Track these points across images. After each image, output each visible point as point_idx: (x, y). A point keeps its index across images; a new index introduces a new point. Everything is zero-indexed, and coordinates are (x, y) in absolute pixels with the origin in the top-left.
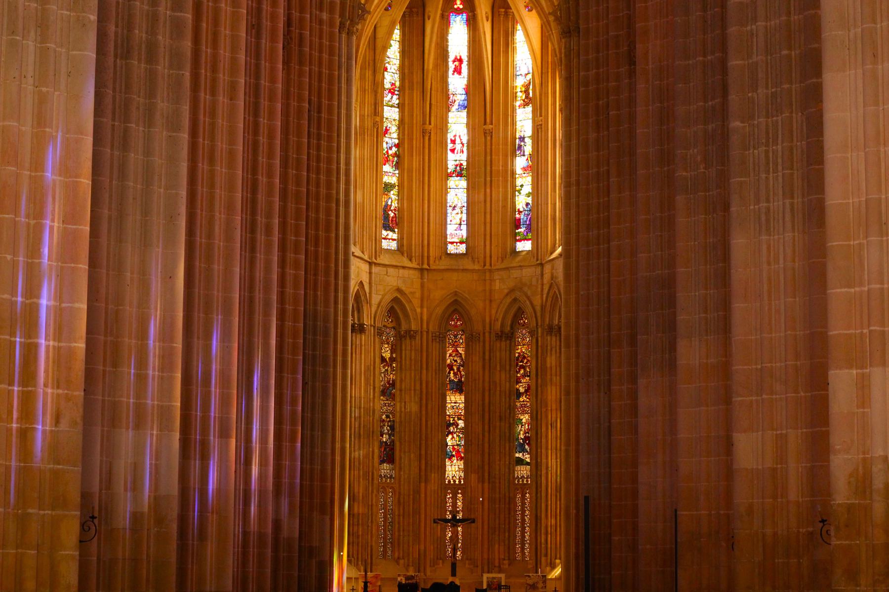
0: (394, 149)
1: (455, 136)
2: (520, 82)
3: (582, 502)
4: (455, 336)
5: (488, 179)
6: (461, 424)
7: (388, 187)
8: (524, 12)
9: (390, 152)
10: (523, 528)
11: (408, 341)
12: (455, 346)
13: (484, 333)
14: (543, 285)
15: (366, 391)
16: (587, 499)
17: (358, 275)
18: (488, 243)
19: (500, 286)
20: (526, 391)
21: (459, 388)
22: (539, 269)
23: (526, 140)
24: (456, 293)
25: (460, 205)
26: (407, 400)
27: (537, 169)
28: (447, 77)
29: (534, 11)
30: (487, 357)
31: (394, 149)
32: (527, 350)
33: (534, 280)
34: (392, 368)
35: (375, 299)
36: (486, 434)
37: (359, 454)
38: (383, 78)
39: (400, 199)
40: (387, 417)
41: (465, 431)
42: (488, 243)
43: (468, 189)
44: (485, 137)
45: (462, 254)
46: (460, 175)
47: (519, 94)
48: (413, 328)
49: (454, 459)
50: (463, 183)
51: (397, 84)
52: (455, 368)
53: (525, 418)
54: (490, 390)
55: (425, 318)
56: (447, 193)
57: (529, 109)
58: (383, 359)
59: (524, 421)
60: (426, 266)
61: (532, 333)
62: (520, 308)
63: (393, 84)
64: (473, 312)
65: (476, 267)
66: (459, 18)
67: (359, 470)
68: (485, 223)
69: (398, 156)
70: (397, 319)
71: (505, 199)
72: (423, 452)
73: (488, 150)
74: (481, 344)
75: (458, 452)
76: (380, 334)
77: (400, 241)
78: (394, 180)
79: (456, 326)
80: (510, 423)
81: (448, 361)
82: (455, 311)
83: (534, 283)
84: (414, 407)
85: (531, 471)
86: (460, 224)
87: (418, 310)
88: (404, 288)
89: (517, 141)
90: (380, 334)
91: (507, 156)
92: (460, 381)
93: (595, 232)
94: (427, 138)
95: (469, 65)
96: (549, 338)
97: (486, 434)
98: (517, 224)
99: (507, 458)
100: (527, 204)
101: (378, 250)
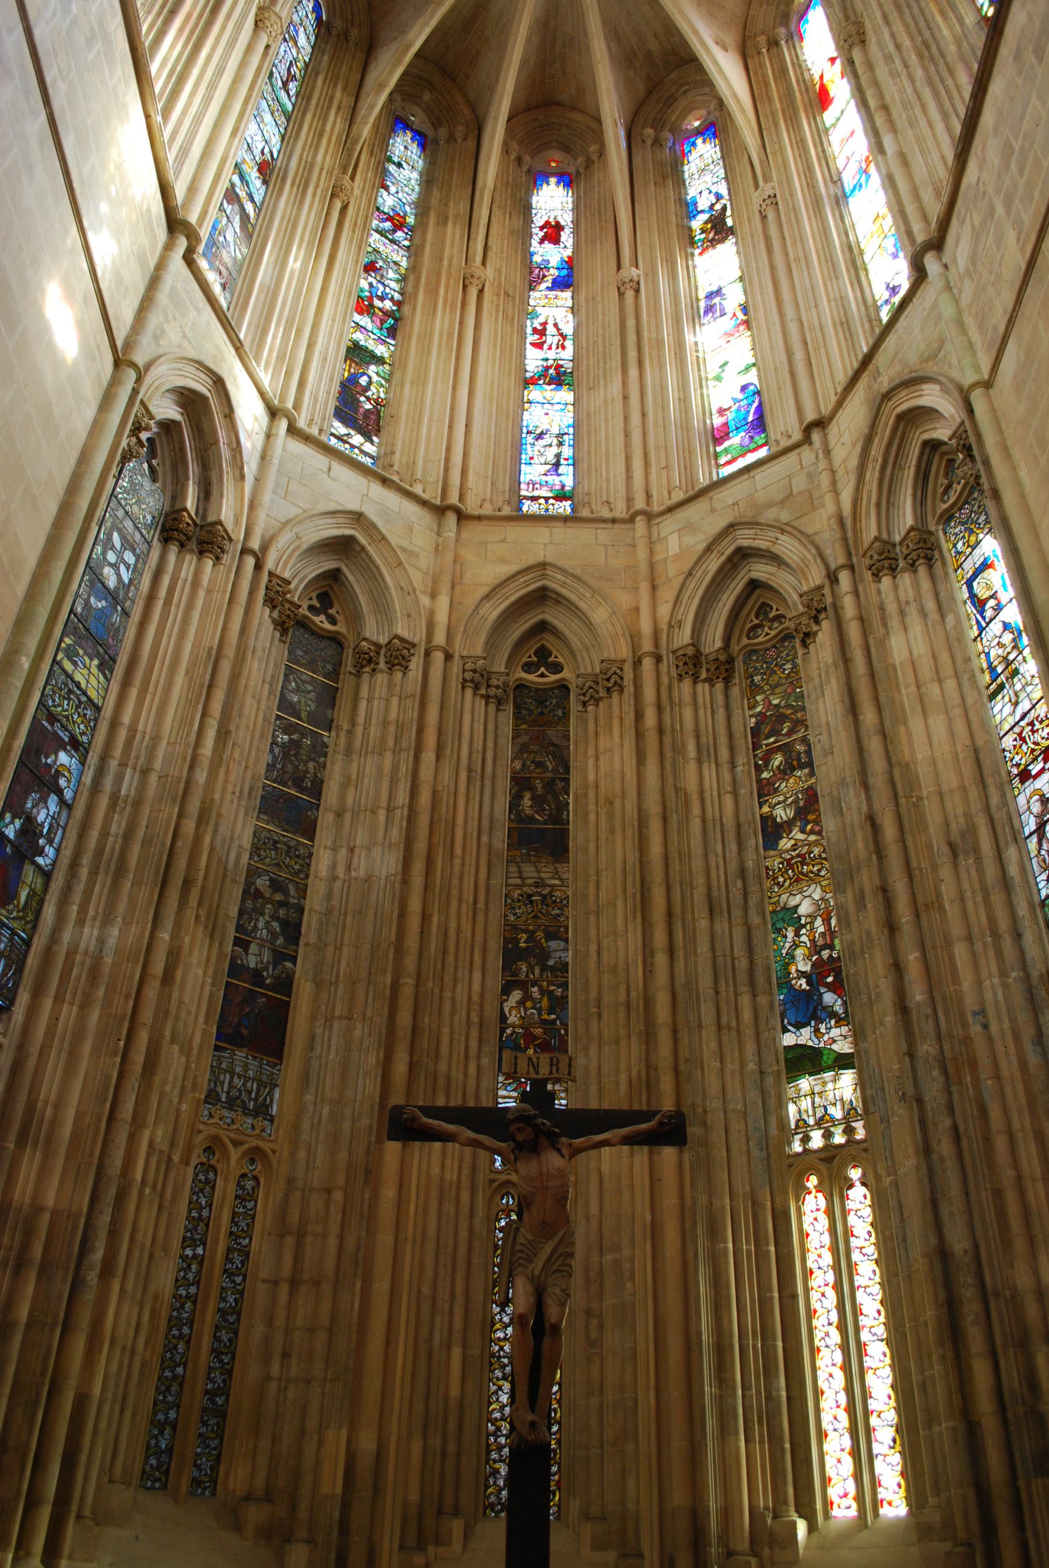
1: (545, 324)
4: (541, 702)
5: (632, 354)
9: (377, 303)
11: (381, 678)
13: (637, 663)
14: (833, 472)
22: (807, 454)
23: (724, 291)
25: (555, 430)
26: (361, 837)
31: (388, 305)
32: (786, 696)
36: (661, 959)
40: (276, 885)
44: (621, 295)
51: (411, 220)
52: (538, 784)
54: (665, 819)
55: (442, 617)
57: (728, 249)
59: (805, 909)
60: (453, 499)
62: (754, 585)
64: (599, 615)
65: (606, 514)
67: (85, 1007)
69: (396, 320)
70: (355, 619)
72: (404, 1019)
73: (630, 310)
74: (629, 690)
78: (380, 350)
80: (749, 929)
83: (799, 484)
86: (557, 465)
87: (425, 601)
89: (702, 304)
94: (473, 292)
96: (886, 581)
97: (661, 959)
99: (750, 1048)
100: (744, 388)
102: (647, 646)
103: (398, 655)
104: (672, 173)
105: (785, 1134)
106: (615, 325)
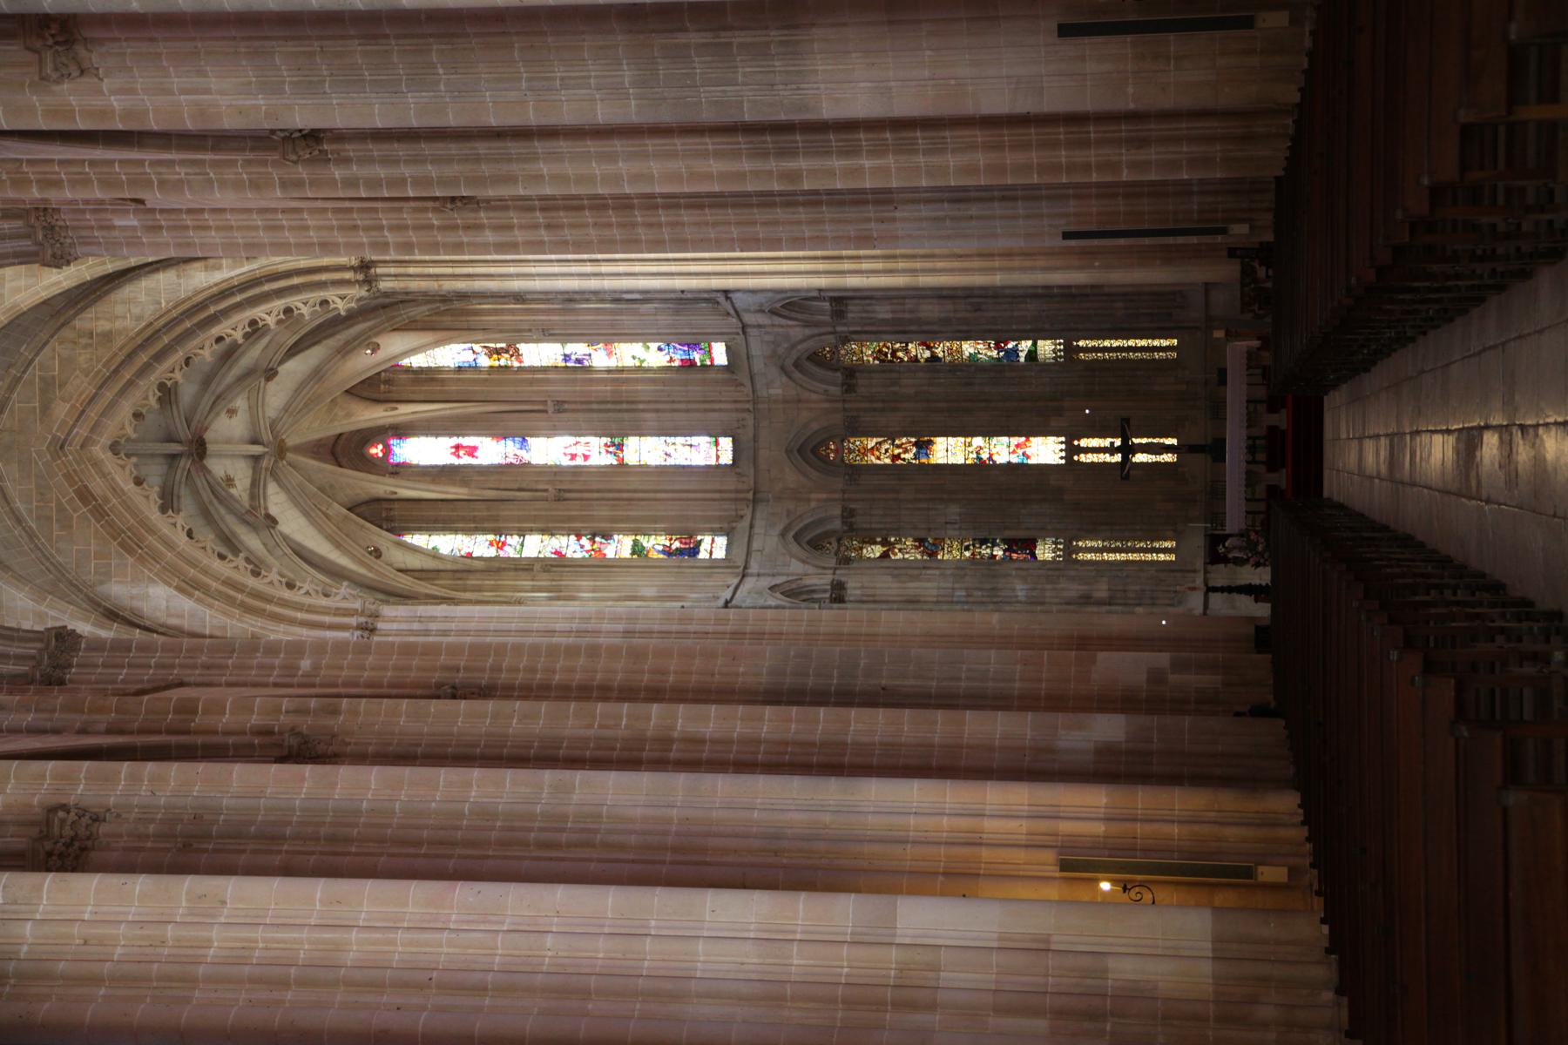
0: (584, 541)
2: (484, 362)
3: (1073, 243)
5: (624, 406)
6: (978, 441)
7: (637, 549)
8: (381, 355)
9: (588, 547)
10: (1130, 349)
12: (866, 451)
13: (845, 410)
15: (929, 580)
16: (1067, 235)
17: (760, 593)
18: (717, 406)
19: (776, 387)
20: (929, 348)
21: (924, 446)
22: (752, 332)
24: (788, 452)
27: (609, 335)
28: (480, 466)
29: (378, 340)
30: (880, 405)
31: (584, 541)
33: (767, 338)
34: (897, 542)
35: (796, 567)
37: (1021, 590)
38: (480, 559)
39: (656, 532)
40: (967, 548)
41: (989, 432)
42: (717, 406)
43: (641, 435)
44: (565, 411)
45: (734, 442)
46: (620, 447)
47: (503, 362)
48: (837, 511)
49: (1028, 451)
50: (632, 443)
51: (491, 537)
52: (897, 451)
53: (968, 348)
56: (647, 466)
57: (522, 347)
58: (885, 555)
59: (972, 351)
60: (750, 496)
61: (846, 340)
62: (808, 358)
63: (491, 544)
64: (815, 426)
65: (750, 422)
66: (396, 450)
68: (687, 411)
69: (594, 535)
70: (827, 535)
71: (653, 381)
75: (1018, 446)
76: (848, 560)
77: (715, 532)
79: (836, 451)
81: (888, 461)
82: (815, 451)
84: (954, 511)
85: (1044, 339)
87: (813, 504)
88: (781, 527)
90: (848, 560)
91: (591, 380)
92: (915, 444)
93: (640, 230)
94: (568, 495)
95: (463, 435)
98: (689, 365)
100: (660, 349)
101: (726, 563)
102: (840, 405)
103: (848, 515)
104: (428, 376)
105: (1056, 363)
106: (595, 415)
